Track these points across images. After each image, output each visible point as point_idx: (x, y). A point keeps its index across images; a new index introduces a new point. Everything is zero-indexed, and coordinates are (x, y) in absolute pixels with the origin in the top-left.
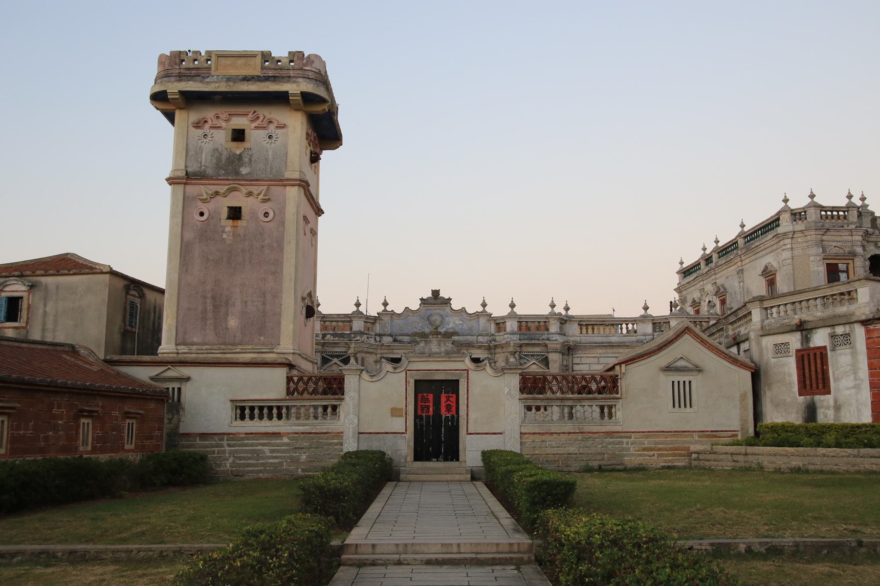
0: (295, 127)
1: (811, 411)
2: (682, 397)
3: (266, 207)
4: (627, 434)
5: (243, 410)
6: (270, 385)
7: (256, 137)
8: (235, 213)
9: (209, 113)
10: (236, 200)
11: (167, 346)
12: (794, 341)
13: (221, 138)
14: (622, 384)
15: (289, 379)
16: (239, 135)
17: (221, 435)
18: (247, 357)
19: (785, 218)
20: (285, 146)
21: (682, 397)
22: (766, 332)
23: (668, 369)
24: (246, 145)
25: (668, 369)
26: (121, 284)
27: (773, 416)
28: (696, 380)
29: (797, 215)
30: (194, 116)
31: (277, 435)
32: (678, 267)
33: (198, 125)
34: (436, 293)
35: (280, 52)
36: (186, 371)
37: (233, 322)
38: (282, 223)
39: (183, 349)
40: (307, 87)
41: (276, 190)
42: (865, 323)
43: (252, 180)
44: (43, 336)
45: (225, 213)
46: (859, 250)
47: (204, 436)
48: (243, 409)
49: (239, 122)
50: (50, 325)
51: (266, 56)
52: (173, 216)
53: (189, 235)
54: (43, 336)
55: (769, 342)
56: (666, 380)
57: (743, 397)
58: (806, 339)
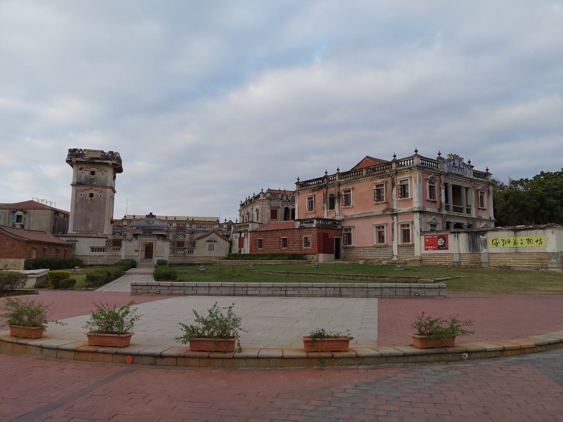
0: (110, 172)
1: (240, 251)
2: (211, 248)
3: (101, 194)
4: (196, 257)
5: (93, 249)
6: (101, 243)
7: (98, 174)
8: (91, 195)
9: (84, 166)
10: (92, 191)
11: (70, 231)
12: (238, 235)
13: (87, 173)
14: (196, 245)
15: (107, 241)
16: (93, 173)
17: (87, 256)
18: (95, 235)
19: (261, 195)
20: (107, 177)
21: (211, 248)
22: (234, 232)
23: (209, 241)
24: (95, 176)
25: (209, 241)
26: (53, 212)
27: (233, 252)
28: (215, 244)
29: (264, 195)
30: (79, 167)
31: (103, 256)
32: (240, 203)
33: (81, 169)
34: (151, 213)
35: (106, 151)
36: (77, 239)
37: (90, 226)
38: (106, 199)
39: (75, 232)
40: (114, 162)
41: (104, 189)
42: (250, 232)
43: (96, 186)
44: (29, 228)
45: (88, 195)
46: (281, 206)
47: (82, 256)
48: (93, 249)
49: (93, 169)
50: (31, 224)
51: (102, 152)
52: (72, 195)
53: (77, 201)
54: (29, 228)
55: (234, 235)
56: (208, 244)
57: (226, 248)
58: (240, 235)
